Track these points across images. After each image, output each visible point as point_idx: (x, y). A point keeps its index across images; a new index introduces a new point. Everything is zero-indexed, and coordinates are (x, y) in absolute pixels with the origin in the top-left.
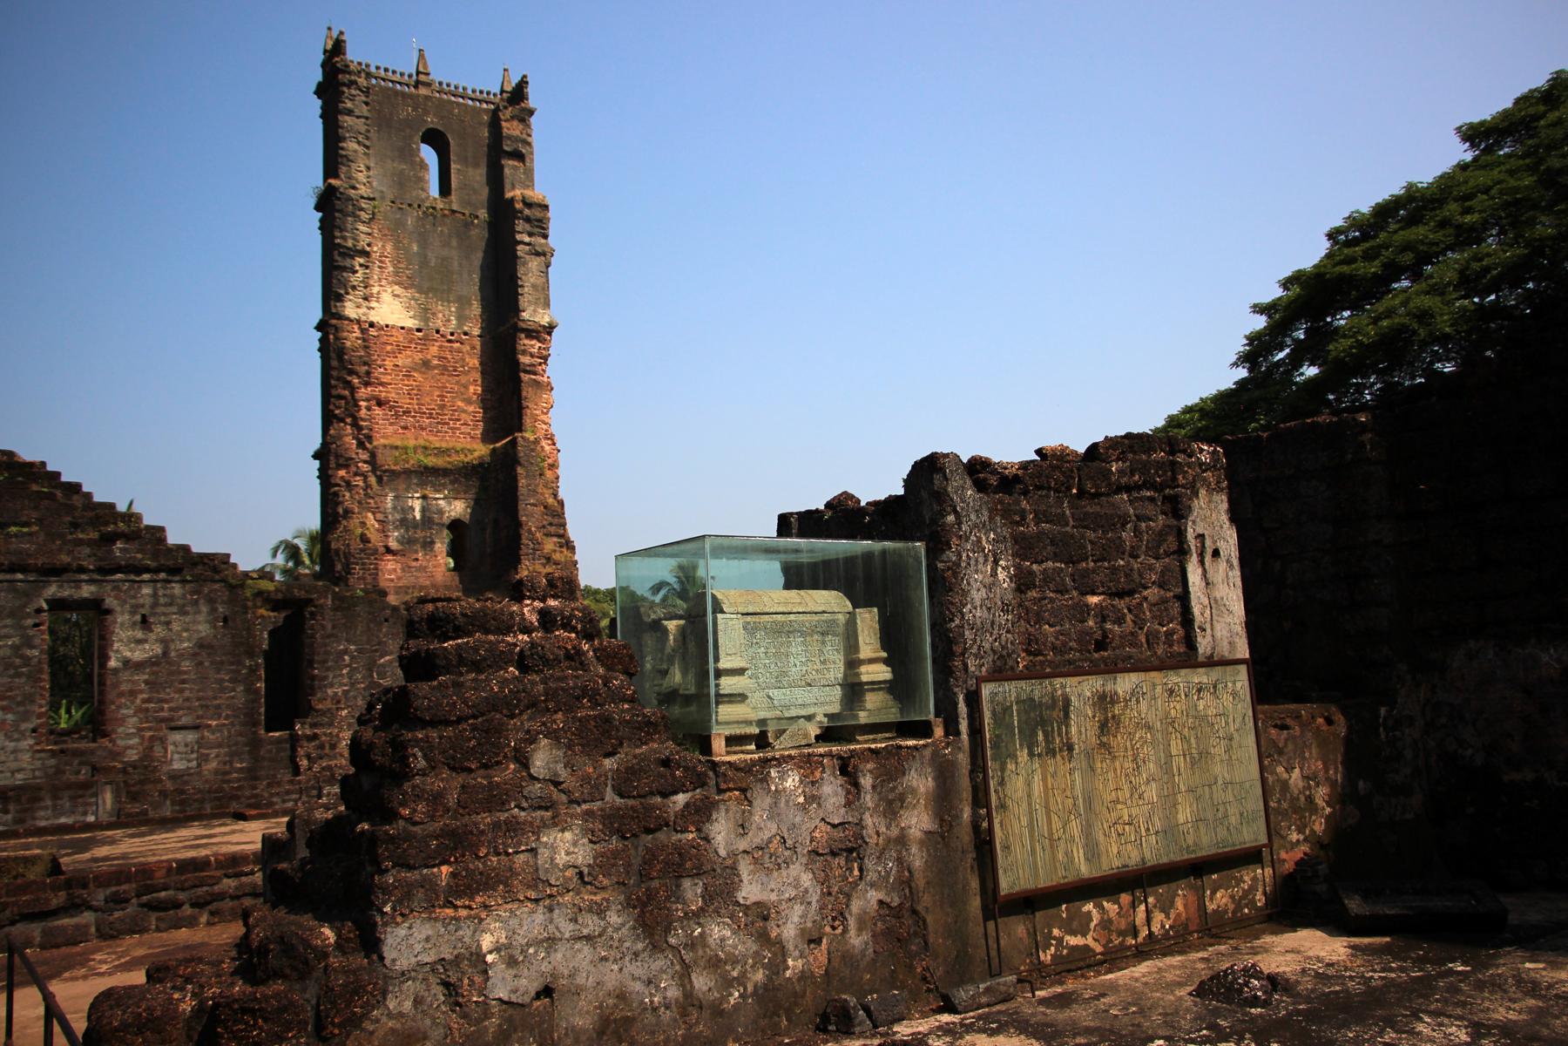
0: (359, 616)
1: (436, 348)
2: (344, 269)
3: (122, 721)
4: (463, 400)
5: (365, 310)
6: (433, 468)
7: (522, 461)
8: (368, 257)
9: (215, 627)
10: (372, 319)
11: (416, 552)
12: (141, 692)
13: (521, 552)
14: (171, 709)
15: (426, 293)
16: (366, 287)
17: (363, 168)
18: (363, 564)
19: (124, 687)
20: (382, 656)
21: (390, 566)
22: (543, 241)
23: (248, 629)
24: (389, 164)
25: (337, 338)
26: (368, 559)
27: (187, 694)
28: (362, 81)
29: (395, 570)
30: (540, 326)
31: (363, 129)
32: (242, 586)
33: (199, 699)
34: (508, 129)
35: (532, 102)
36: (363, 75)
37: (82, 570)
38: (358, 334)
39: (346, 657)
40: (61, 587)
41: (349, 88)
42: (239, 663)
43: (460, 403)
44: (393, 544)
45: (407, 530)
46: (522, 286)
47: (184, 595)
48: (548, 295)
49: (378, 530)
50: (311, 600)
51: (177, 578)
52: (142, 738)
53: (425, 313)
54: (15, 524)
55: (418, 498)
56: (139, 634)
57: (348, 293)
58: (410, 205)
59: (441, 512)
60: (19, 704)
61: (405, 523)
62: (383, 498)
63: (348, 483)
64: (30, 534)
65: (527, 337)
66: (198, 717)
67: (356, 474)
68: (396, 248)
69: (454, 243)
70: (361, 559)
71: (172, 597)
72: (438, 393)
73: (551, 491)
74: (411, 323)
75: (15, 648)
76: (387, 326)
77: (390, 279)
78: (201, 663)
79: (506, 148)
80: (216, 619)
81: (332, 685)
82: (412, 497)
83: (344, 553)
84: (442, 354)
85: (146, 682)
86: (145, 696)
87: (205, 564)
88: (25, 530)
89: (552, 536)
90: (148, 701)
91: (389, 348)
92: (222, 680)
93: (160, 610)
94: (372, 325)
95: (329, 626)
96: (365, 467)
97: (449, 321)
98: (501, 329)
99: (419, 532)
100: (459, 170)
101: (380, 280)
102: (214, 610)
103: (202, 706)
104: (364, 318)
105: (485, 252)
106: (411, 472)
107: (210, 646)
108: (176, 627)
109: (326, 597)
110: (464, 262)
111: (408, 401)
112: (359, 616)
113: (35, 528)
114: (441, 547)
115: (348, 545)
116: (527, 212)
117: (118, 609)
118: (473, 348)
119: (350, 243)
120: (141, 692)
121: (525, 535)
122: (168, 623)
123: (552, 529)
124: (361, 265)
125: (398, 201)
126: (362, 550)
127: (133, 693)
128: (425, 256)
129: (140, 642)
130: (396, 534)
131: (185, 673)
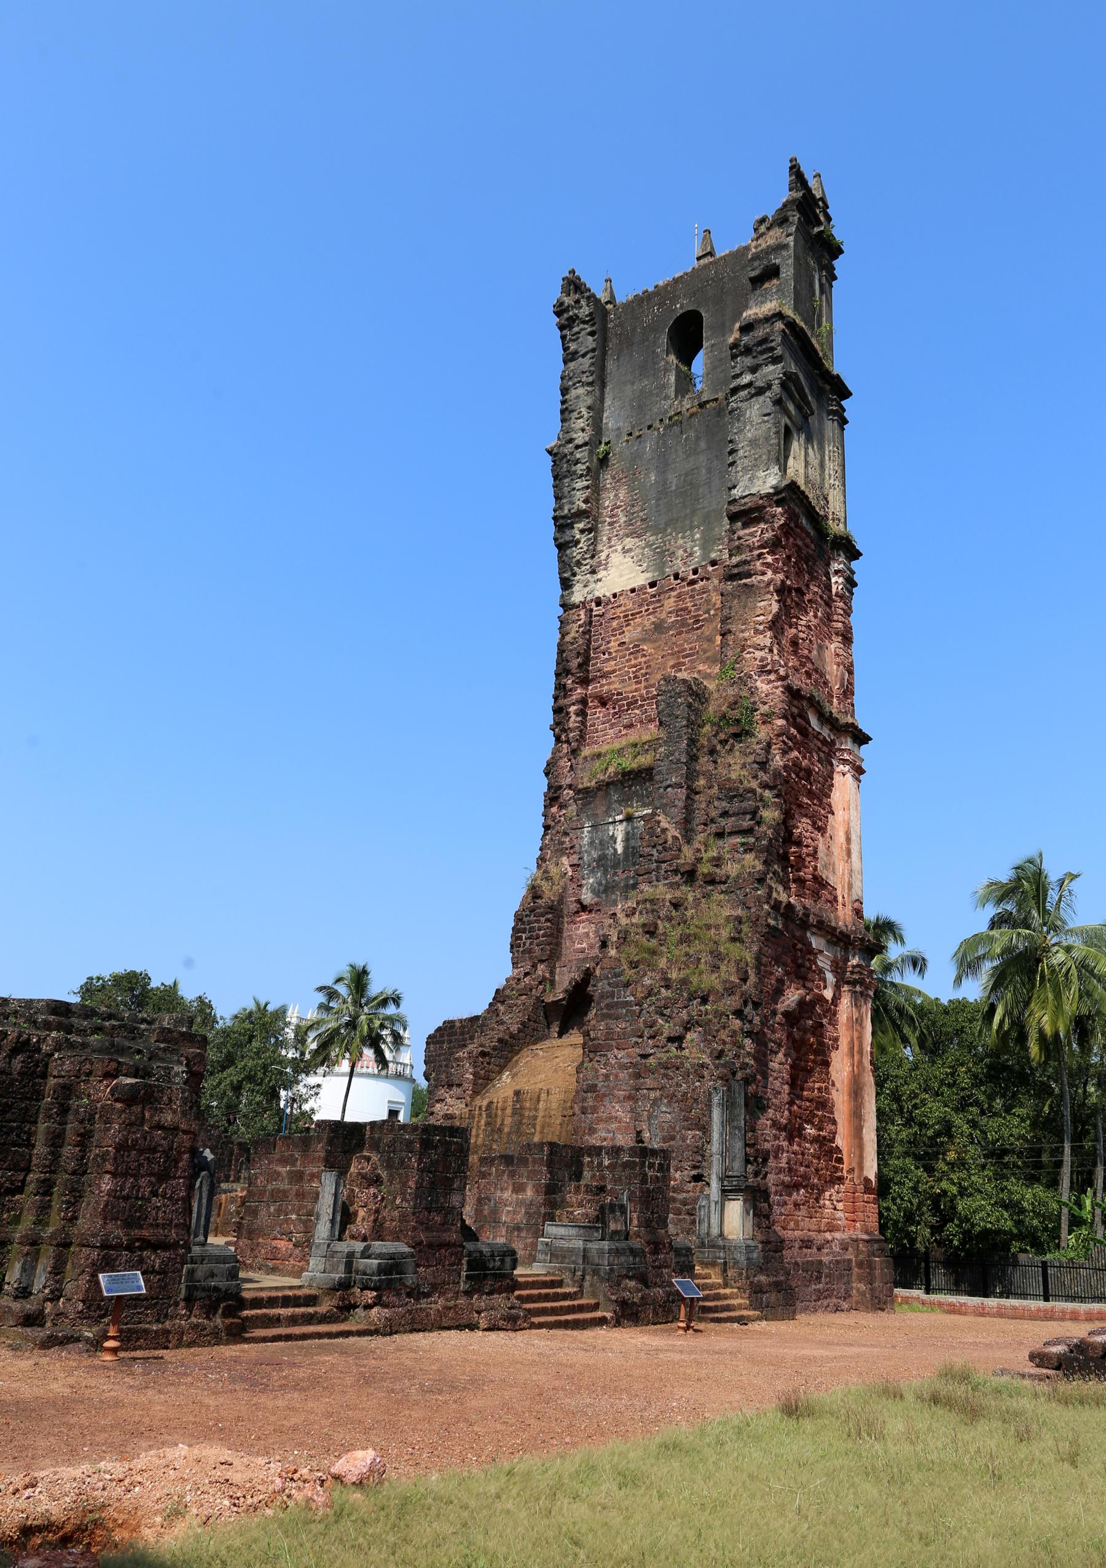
8: (588, 517)
10: (597, 594)
11: (615, 903)
16: (593, 557)
18: (532, 930)
26: (538, 921)
29: (587, 935)
30: (761, 498)
43: (701, 667)
44: (587, 897)
55: (621, 821)
57: (574, 575)
62: (579, 831)
65: (745, 526)
68: (631, 490)
70: (529, 923)
72: (671, 663)
76: (615, 596)
77: (621, 533)
82: (614, 822)
84: (681, 605)
89: (731, 834)
91: (615, 624)
94: (598, 602)
99: (620, 871)
100: (713, 346)
101: (609, 539)
106: (608, 784)
111: (634, 687)
123: (729, 824)
124: (582, 531)
130: (591, 881)
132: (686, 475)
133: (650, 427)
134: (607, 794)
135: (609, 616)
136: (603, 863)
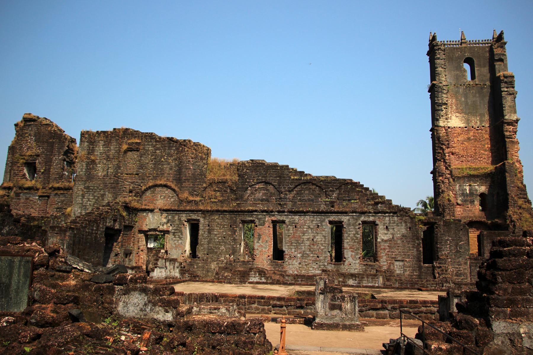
0: (452, 228)
1: (472, 133)
2: (439, 110)
3: (382, 257)
4: (483, 150)
5: (446, 123)
6: (473, 175)
7: (508, 171)
9: (407, 230)
10: (449, 126)
11: (468, 204)
12: (387, 249)
13: (509, 205)
14: (395, 255)
15: (468, 114)
17: (444, 76)
18: (449, 209)
19: (382, 247)
20: (460, 242)
21: (459, 209)
22: (512, 89)
23: (417, 231)
24: (453, 73)
25: (437, 133)
27: (399, 250)
28: (442, 47)
29: (460, 211)
31: (443, 63)
32: (415, 218)
33: (403, 252)
34: (496, 51)
35: (505, 40)
36: (443, 45)
37: (370, 213)
38: (444, 131)
39: (448, 242)
40: (365, 217)
41: (438, 51)
42: (415, 242)
43: (482, 151)
44: (459, 202)
45: (464, 197)
46: (505, 107)
47: (398, 220)
48: (515, 109)
49: (454, 197)
50: (436, 223)
51: (395, 215)
52: (388, 262)
53: (468, 121)
54: (353, 200)
56: (386, 232)
57: (440, 118)
58: (461, 85)
59: (476, 190)
60: (355, 250)
61: (463, 194)
63: (443, 182)
64: (357, 202)
65: (507, 125)
66: (403, 258)
67: (445, 178)
68: (457, 100)
69: (477, 95)
71: (394, 221)
73: (520, 181)
74: (462, 125)
75: (354, 234)
76: (454, 127)
78: (403, 241)
79: (496, 58)
80: (407, 228)
81: (444, 251)
83: (442, 205)
85: (388, 246)
86: (388, 250)
87: (403, 211)
88: (355, 201)
90: (389, 252)
91: (455, 135)
92: (410, 247)
93: (391, 225)
94: (449, 128)
95: (442, 231)
96: (449, 176)
97: (477, 123)
98: (497, 123)
101: (451, 112)
102: (406, 225)
103: (404, 254)
104: (446, 126)
105: (489, 97)
107: (406, 236)
108: (395, 230)
109: (441, 222)
110: (482, 101)
112: (452, 228)
113: (358, 201)
114: (477, 203)
115: (444, 202)
116: (505, 80)
117: (380, 224)
118: (486, 131)
119: (440, 102)
120: (387, 249)
121: (510, 198)
122: (393, 229)
123: (521, 196)
124: (444, 108)
125: (456, 85)
126: (448, 204)
127: (384, 249)
128: (467, 102)
129: (386, 234)
131: (399, 244)
132: (473, 102)
133: (461, 85)
134: (464, 179)
135: (453, 132)
136: (463, 194)
